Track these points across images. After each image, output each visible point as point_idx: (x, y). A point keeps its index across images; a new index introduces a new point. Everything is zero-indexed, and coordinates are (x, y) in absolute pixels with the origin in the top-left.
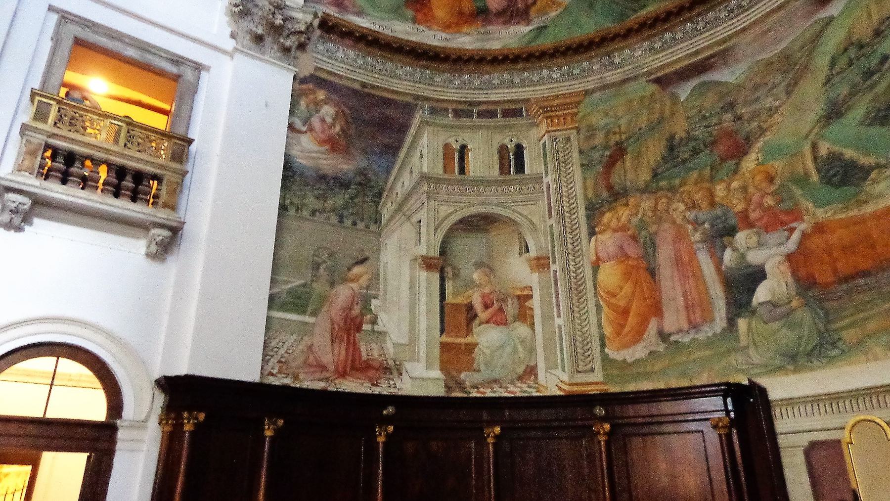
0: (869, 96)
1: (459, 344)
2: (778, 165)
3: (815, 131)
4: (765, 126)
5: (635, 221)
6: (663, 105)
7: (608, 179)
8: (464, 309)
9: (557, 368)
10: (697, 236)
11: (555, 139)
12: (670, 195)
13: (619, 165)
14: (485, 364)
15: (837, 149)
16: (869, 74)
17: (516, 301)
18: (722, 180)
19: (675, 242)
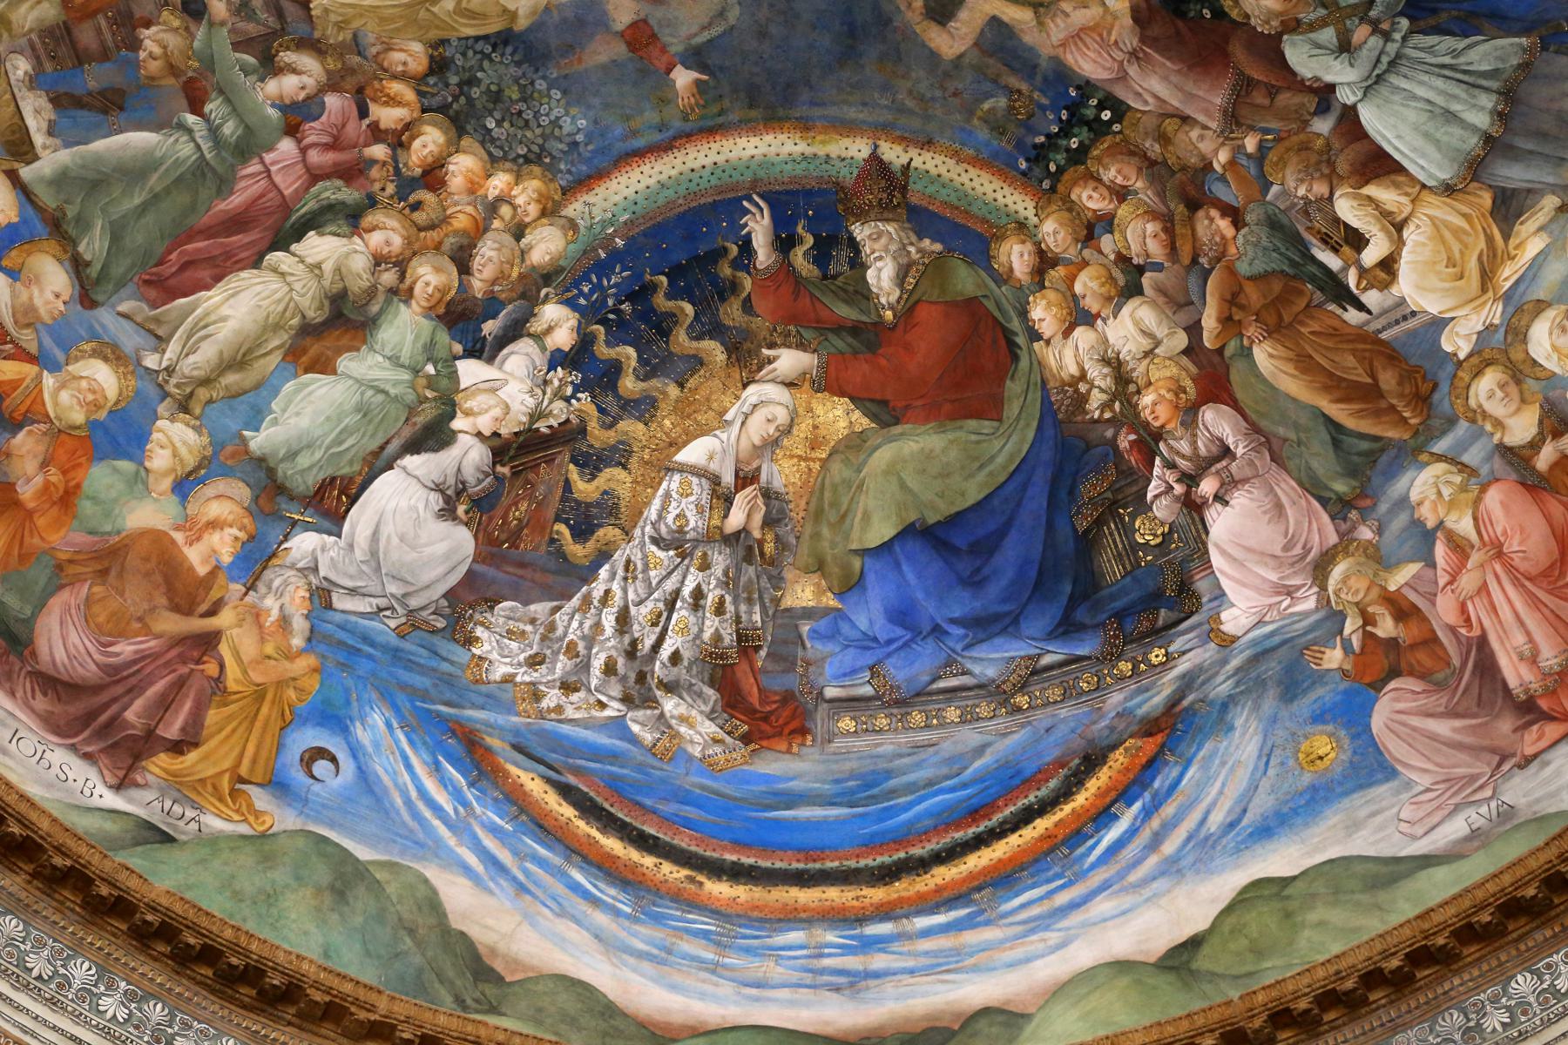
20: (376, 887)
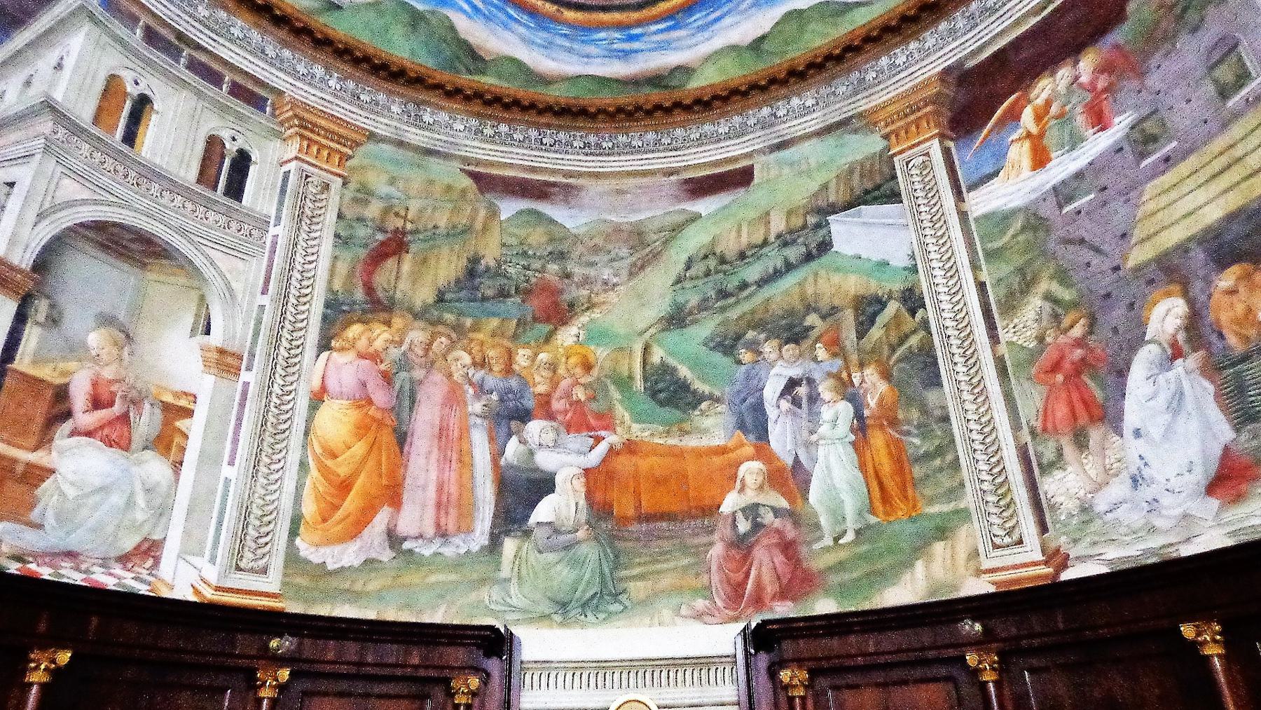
0: (718, 318)
1: (15, 461)
2: (600, 354)
3: (652, 331)
4: (595, 299)
5: (395, 353)
6: (475, 211)
7: (370, 274)
8: (49, 394)
9: (201, 554)
10: (477, 407)
11: (307, 177)
12: (454, 335)
13: (391, 263)
14: (58, 518)
15: (672, 362)
16: (723, 294)
17: (158, 411)
18: (527, 345)
19: (444, 405)
20: (428, 23)
